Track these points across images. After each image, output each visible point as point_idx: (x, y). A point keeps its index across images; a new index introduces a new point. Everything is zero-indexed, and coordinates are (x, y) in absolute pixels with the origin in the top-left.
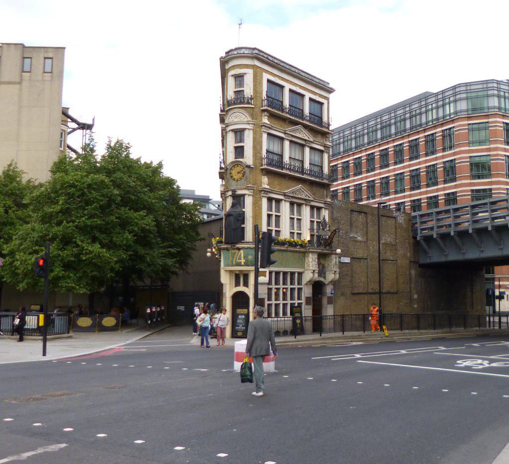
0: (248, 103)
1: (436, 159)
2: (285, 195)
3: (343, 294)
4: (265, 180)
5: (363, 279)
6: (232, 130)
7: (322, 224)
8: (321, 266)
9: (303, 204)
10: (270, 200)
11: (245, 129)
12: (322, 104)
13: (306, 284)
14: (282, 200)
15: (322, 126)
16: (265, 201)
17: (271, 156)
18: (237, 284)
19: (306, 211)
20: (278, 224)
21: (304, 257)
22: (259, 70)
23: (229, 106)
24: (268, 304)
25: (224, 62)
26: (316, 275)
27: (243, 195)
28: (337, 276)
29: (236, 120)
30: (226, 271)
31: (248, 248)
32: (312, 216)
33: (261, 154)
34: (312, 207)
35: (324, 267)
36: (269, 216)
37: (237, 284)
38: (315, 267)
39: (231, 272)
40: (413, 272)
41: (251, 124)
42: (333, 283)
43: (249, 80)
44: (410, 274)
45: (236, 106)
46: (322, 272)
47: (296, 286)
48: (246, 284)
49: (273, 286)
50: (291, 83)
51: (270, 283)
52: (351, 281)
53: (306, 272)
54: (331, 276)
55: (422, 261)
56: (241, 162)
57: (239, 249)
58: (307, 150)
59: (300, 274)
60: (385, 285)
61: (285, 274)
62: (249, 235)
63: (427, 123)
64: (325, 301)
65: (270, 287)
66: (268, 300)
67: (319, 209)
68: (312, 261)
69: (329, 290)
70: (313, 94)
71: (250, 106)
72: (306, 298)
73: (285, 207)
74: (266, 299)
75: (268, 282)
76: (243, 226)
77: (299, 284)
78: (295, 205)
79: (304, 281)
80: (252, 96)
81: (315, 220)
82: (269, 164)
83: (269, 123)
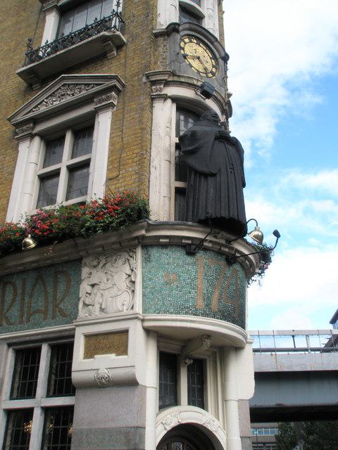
30: (148, 331)
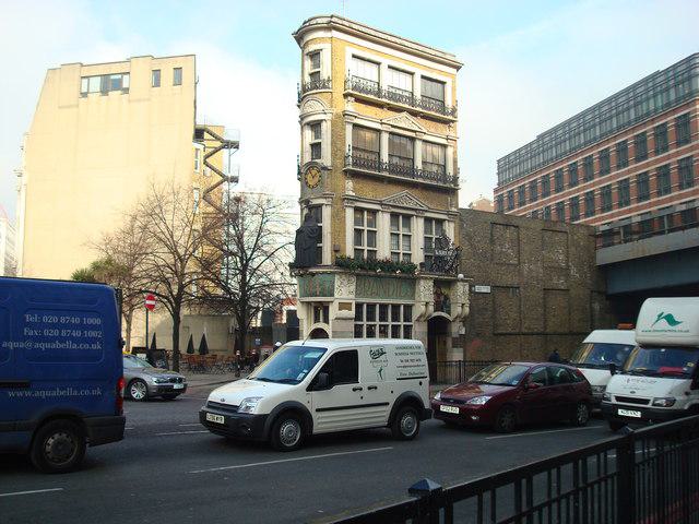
0: (324, 87)
1: (669, 157)
2: (381, 204)
3: (478, 335)
4: (350, 184)
5: (514, 315)
6: (308, 124)
7: (442, 242)
8: (442, 299)
9: (410, 216)
10: (358, 210)
11: (322, 121)
12: (443, 83)
14: (378, 211)
16: (350, 214)
17: (358, 153)
18: (317, 320)
19: (418, 226)
20: (372, 241)
21: (414, 289)
25: (300, 37)
26: (431, 308)
27: (320, 206)
28: (467, 310)
31: (323, 273)
32: (427, 230)
33: (344, 151)
34: (428, 220)
35: (447, 298)
36: (358, 232)
37: (317, 320)
38: (431, 299)
39: (309, 303)
40: (597, 306)
42: (464, 320)
43: (325, 58)
44: (592, 309)
46: (442, 303)
47: (402, 323)
48: (326, 320)
49: (365, 323)
51: (358, 317)
52: (493, 317)
53: (417, 305)
54: (457, 310)
55: (610, 292)
56: (317, 163)
57: (313, 275)
58: (419, 144)
59: (408, 308)
60: (550, 324)
61: (383, 307)
62: (327, 258)
63: (656, 110)
64: (450, 343)
67: (440, 222)
68: (425, 291)
69: (458, 329)
73: (384, 220)
78: (401, 217)
79: (414, 317)
81: (434, 236)
82: (354, 164)
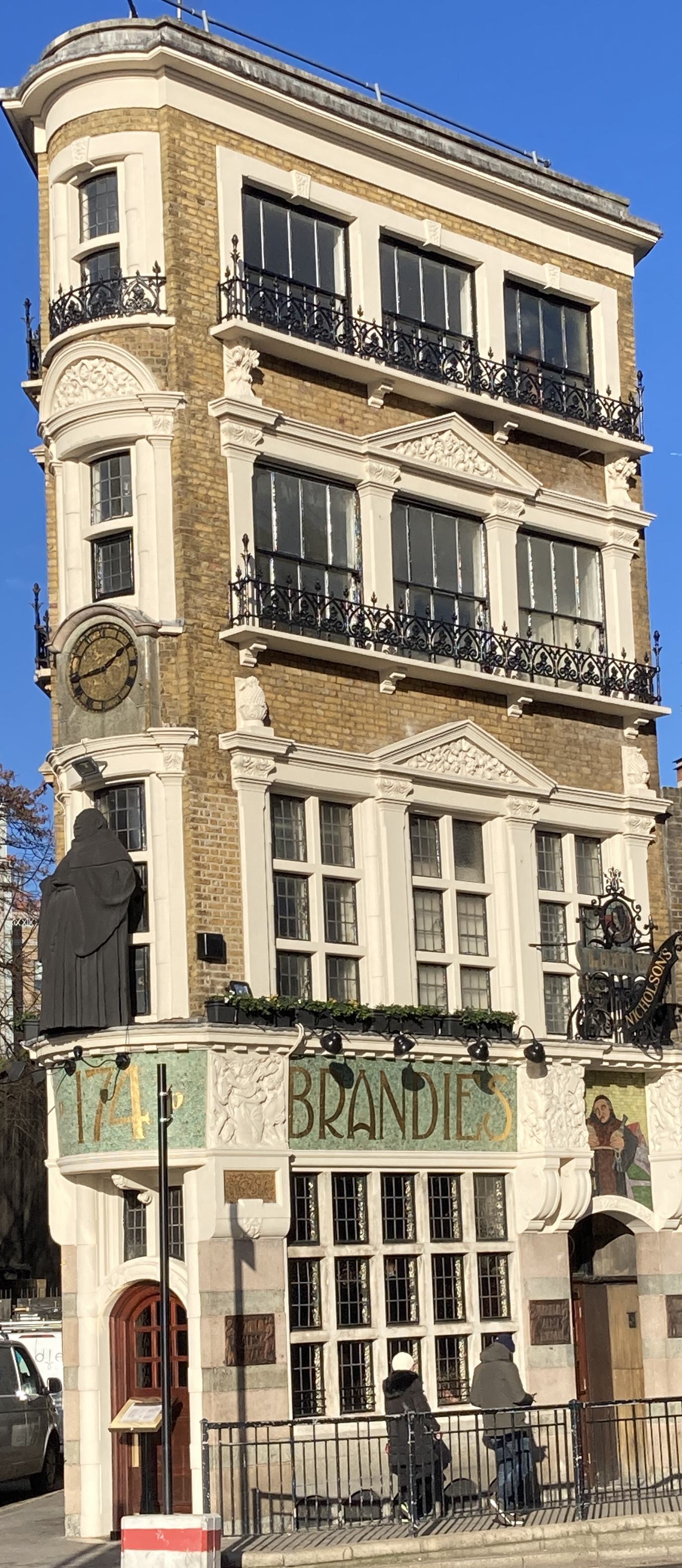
8: (618, 1141)
13: (530, 1234)
15: (594, 422)
22: (189, 131)
23: (56, 331)
24: (295, 1348)
29: (87, 398)
41: (159, 409)
45: (82, 328)
50: (391, 198)
65: (304, 1252)
66: (294, 1325)
70: (532, 258)
71: (152, 318)
72: (534, 1304)
74: (283, 1323)
75: (285, 1225)
76: (138, 938)
77: (483, 1234)
80: (157, 269)
83: (258, 402)
